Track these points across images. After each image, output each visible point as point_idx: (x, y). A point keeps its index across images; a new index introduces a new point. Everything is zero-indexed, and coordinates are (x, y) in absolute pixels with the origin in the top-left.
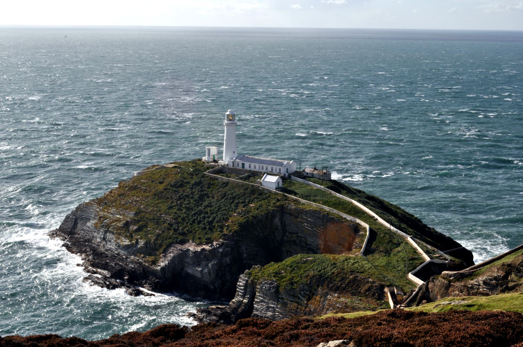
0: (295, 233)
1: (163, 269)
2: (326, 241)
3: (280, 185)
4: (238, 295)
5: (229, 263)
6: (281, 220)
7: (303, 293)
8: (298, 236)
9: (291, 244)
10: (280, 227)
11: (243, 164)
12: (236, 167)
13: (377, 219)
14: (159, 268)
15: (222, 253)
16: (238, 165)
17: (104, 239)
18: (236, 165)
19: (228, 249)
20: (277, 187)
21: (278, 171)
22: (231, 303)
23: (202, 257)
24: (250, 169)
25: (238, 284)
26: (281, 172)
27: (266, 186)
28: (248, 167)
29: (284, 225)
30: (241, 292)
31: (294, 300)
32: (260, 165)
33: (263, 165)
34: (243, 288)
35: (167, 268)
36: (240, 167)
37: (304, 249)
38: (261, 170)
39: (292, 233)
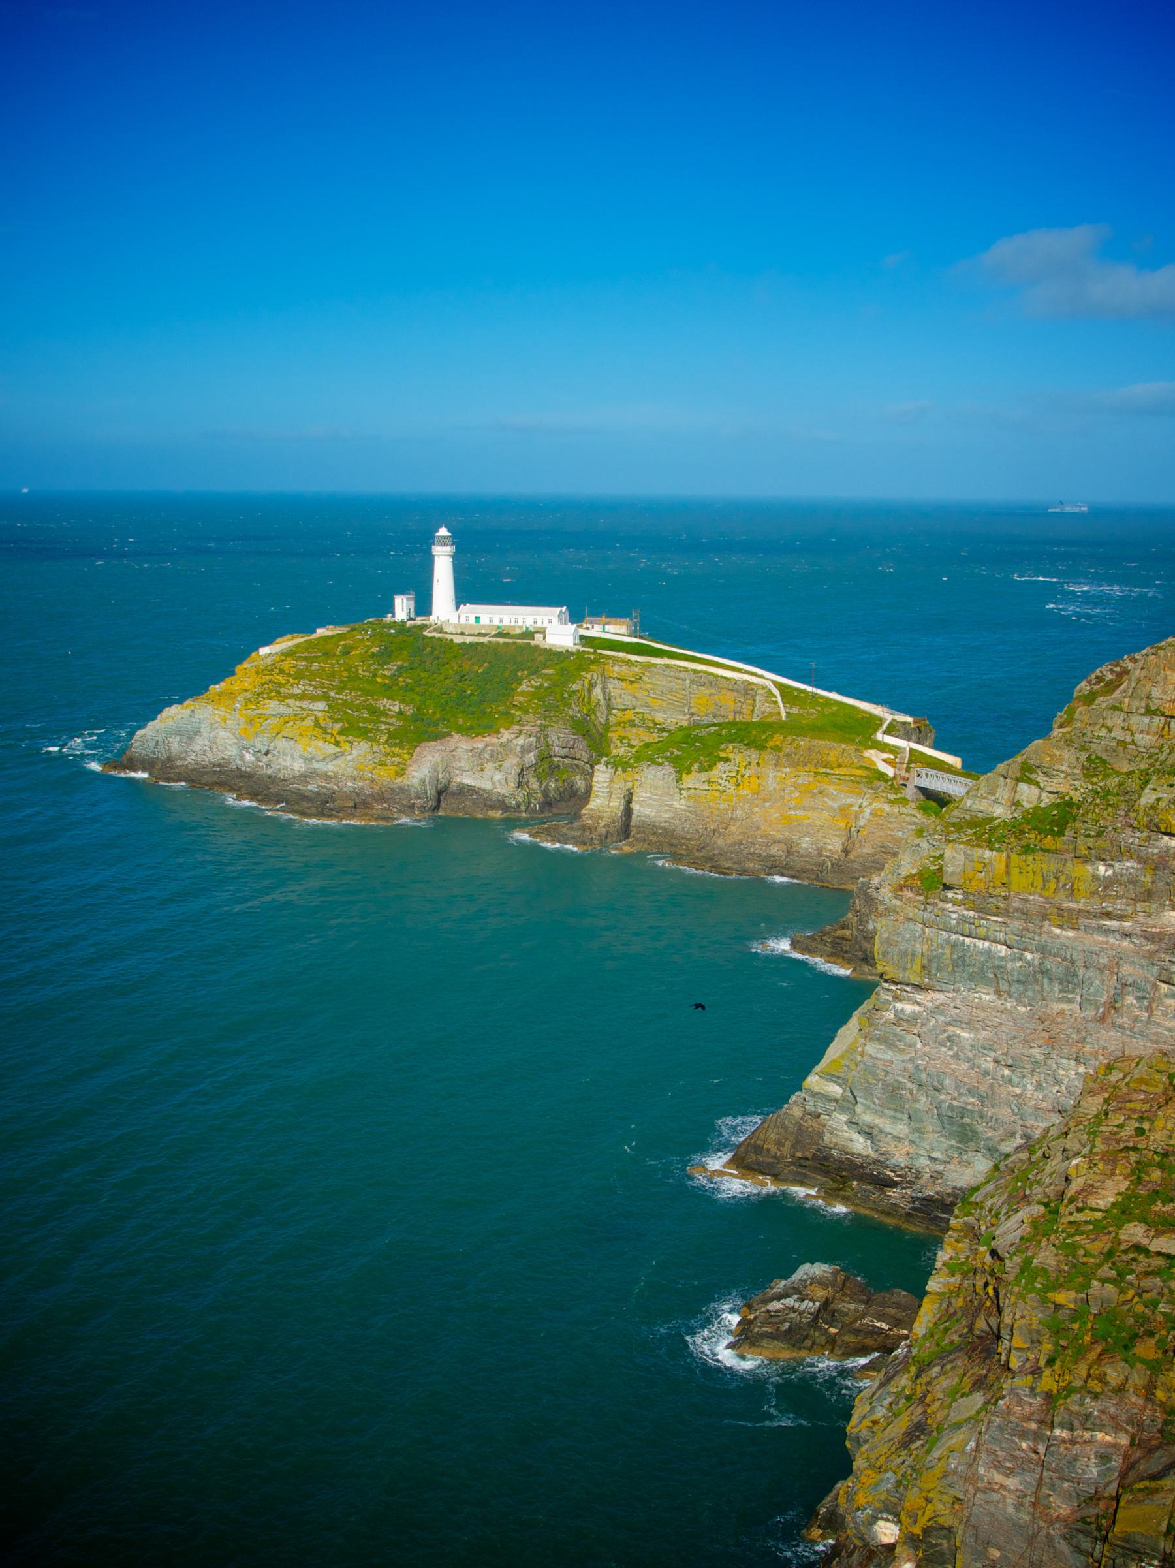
0: (630, 709)
1: (423, 781)
2: (692, 714)
4: (597, 796)
5: (534, 762)
6: (604, 689)
7: (724, 776)
8: (637, 713)
9: (625, 727)
10: (602, 702)
14: (415, 782)
19: (531, 739)
22: (583, 812)
23: (487, 756)
25: (595, 779)
29: (608, 700)
30: (603, 792)
31: (710, 788)
32: (511, 616)
33: (516, 617)
34: (606, 785)
35: (427, 780)
37: (652, 730)
39: (626, 710)
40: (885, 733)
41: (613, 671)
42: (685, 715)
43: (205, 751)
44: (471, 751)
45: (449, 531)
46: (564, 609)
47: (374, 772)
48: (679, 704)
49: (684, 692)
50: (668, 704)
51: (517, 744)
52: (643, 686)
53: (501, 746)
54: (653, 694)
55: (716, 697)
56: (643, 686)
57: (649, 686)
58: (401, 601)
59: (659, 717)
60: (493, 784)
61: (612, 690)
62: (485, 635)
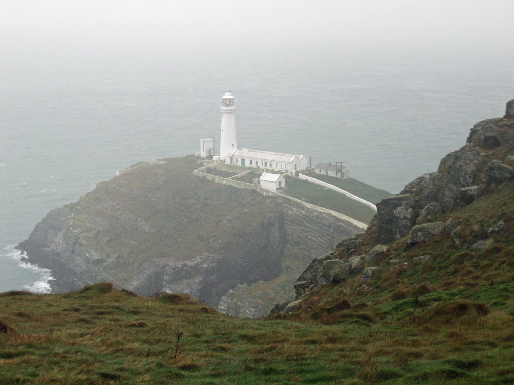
3: (283, 185)
9: (292, 259)
11: (243, 160)
12: (235, 163)
15: (206, 269)
16: (237, 161)
17: (73, 252)
18: (234, 160)
20: (278, 187)
21: (284, 168)
24: (251, 166)
26: (288, 169)
27: (264, 185)
28: (249, 163)
36: (240, 163)
38: (263, 167)
41: (288, 215)
43: (59, 243)
44: (174, 269)
45: (232, 95)
47: (115, 277)
48: (325, 246)
49: (329, 237)
53: (191, 267)
54: (310, 235)
57: (308, 229)
58: (202, 143)
61: (287, 229)
62: (226, 175)
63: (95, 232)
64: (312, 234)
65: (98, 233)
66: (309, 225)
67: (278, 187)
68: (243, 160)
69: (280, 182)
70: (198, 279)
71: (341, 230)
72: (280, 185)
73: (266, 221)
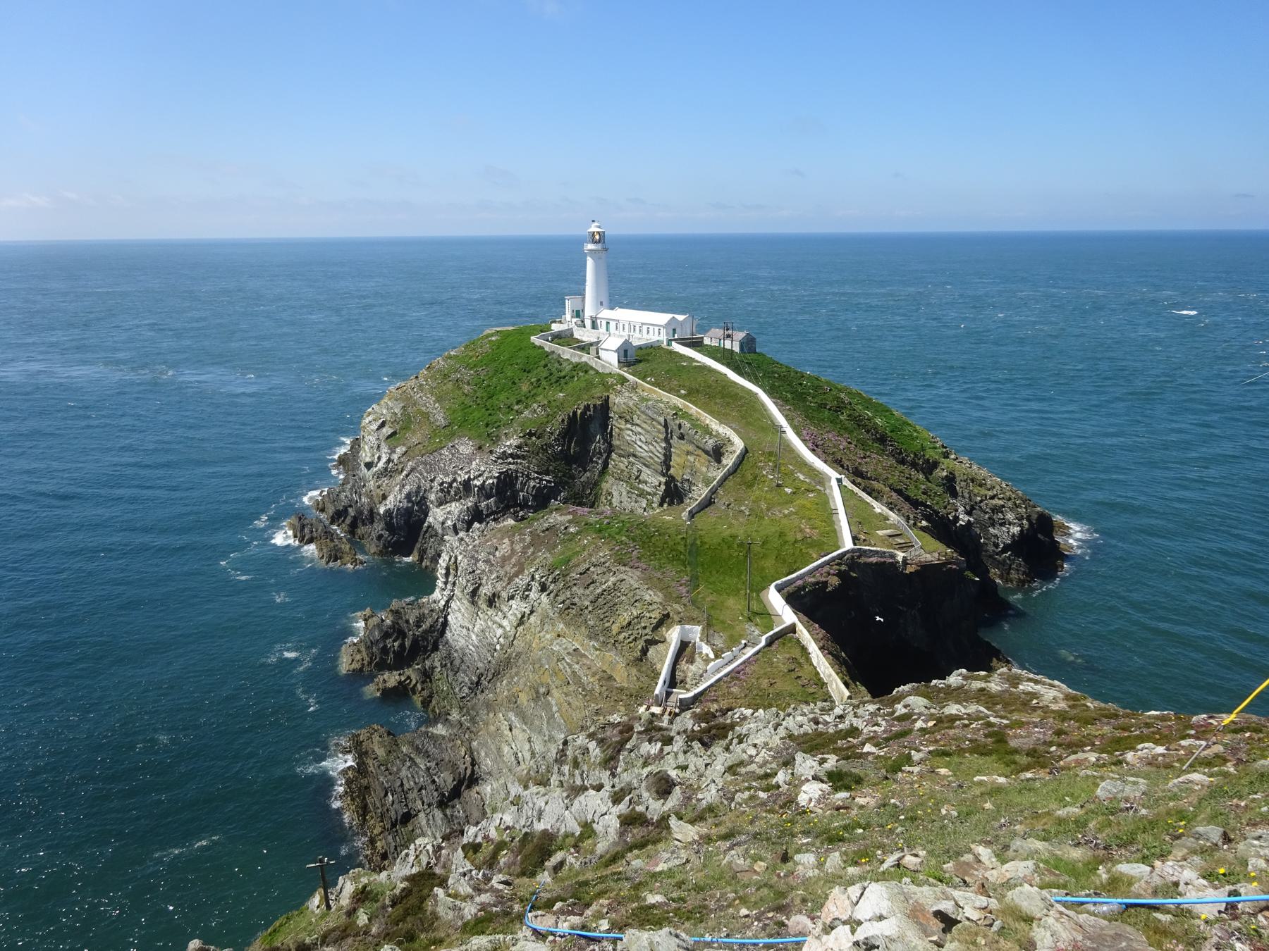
1: (389, 513)
2: (671, 479)
8: (629, 462)
11: (608, 323)
13: (784, 432)
15: (482, 487)
23: (453, 493)
40: (779, 589)
42: (664, 475)
46: (680, 318)
48: (656, 459)
50: (650, 457)
51: (476, 486)
52: (633, 428)
54: (640, 440)
55: (691, 458)
56: (633, 428)
57: (639, 429)
59: (646, 474)
60: (443, 529)
63: (381, 421)
64: (643, 439)
65: (383, 425)
66: (638, 422)
67: (623, 359)
68: (608, 323)
69: (626, 351)
70: (470, 502)
71: (681, 433)
72: (626, 356)
73: (579, 412)
